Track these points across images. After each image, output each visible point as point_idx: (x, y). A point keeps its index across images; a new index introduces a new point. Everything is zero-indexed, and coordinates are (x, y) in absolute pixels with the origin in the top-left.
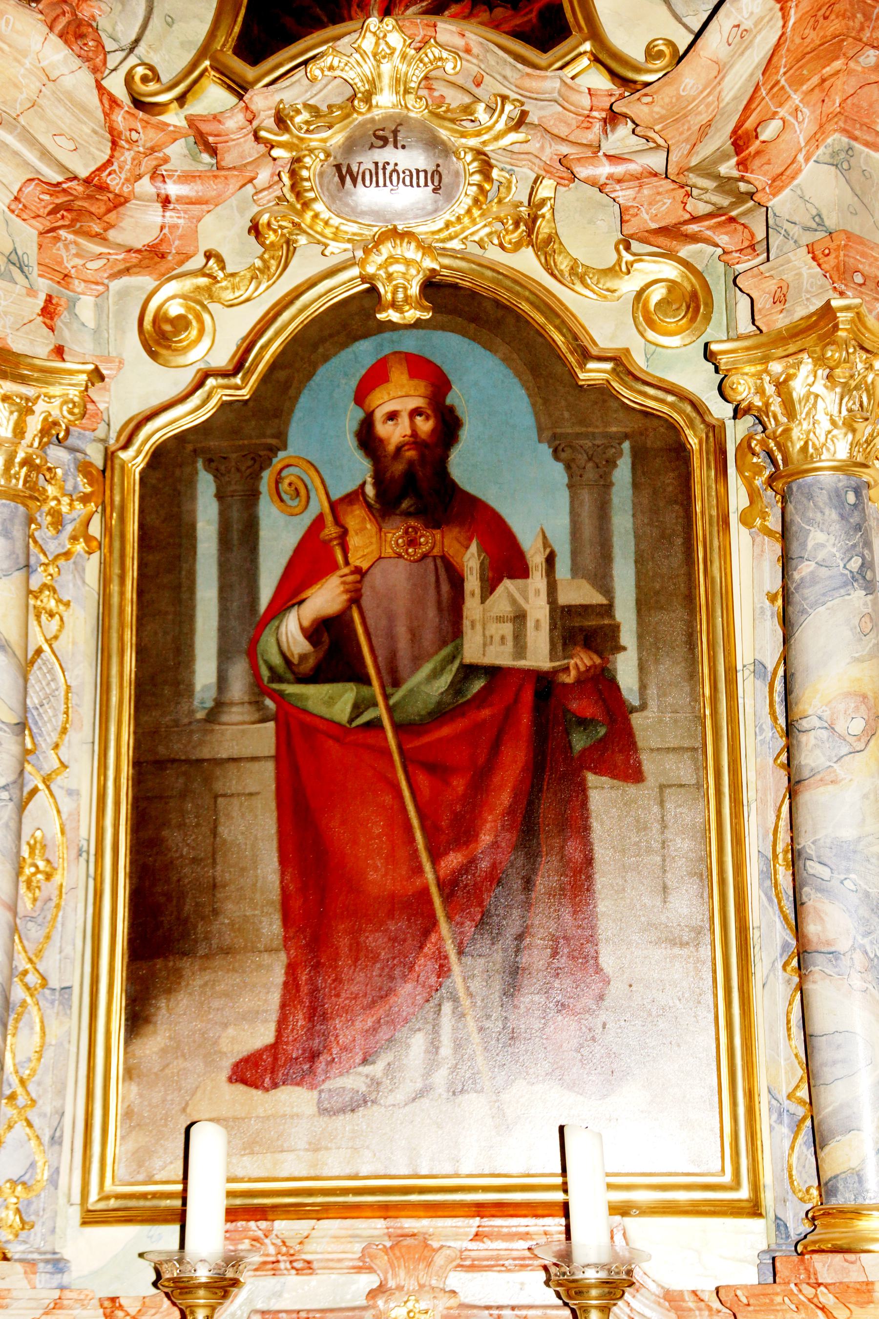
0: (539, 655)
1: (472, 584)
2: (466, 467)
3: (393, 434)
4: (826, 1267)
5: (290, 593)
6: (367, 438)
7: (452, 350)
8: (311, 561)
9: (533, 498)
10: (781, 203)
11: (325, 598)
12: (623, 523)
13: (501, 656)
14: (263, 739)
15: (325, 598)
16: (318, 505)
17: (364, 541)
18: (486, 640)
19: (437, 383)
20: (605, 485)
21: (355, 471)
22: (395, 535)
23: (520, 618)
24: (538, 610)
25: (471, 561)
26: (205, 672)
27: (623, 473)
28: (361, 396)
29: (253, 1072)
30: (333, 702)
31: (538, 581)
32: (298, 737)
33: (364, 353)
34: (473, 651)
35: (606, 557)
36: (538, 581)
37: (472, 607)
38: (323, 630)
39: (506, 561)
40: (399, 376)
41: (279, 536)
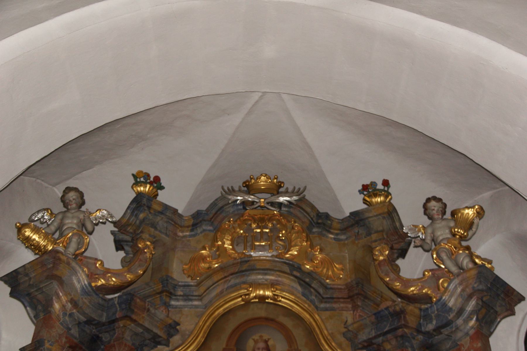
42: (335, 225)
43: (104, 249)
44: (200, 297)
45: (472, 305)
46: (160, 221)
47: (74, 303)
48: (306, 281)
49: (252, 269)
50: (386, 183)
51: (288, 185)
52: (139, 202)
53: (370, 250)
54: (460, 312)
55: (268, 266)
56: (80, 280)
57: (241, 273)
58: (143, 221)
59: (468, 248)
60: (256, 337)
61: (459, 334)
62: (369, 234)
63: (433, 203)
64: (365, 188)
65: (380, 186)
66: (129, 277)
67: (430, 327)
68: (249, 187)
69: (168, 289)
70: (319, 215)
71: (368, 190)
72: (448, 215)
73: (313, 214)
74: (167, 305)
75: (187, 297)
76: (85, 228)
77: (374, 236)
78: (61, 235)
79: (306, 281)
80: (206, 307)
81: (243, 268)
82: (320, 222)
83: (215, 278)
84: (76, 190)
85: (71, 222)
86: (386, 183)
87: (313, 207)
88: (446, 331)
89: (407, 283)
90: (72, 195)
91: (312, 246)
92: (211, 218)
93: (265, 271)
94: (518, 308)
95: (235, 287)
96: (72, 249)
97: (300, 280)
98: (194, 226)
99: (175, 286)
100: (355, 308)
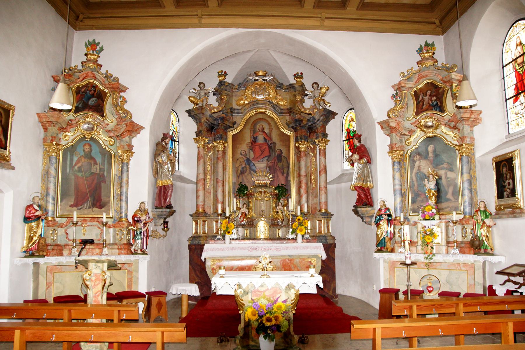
0: (98, 172)
1: (93, 165)
2: (93, 154)
3: (86, 150)
4: (120, 222)
5: (76, 165)
6: (84, 150)
7: (92, 143)
8: (78, 161)
9: (99, 159)
10: (124, 139)
11: (79, 165)
12: (106, 161)
13: (95, 172)
14: (73, 177)
15: (79, 165)
16: (79, 156)
17: (83, 160)
18: (93, 170)
19: (91, 146)
20: (105, 157)
21: (82, 153)
22: (86, 160)
23: (96, 169)
24: (98, 168)
25: (93, 163)
26: (68, 170)
27: (106, 156)
28: (84, 146)
29: (72, 206)
30: (80, 174)
31: (98, 165)
32: (77, 177)
33: (84, 143)
34: (92, 171)
35: (104, 164)
36: (98, 165)
37: (93, 167)
38: (79, 168)
39: (96, 163)
40: (87, 145)
41: (75, 159)
42: (285, 87)
43: (213, 101)
44: (242, 113)
45: (321, 118)
46: (228, 88)
47: (208, 120)
48: (275, 107)
49: (258, 104)
50: (302, 73)
51: (270, 73)
52: (221, 83)
53: (295, 96)
54: (318, 120)
55: (263, 102)
56: (208, 113)
57: (254, 105)
58: (222, 89)
59: (324, 100)
60: (260, 124)
61: (318, 126)
62: (295, 91)
63: (314, 85)
64: (295, 75)
65: (300, 74)
66: (220, 108)
67: (310, 124)
68: (256, 74)
69: (232, 110)
70: (279, 84)
71: (296, 76)
72: (319, 88)
73: (278, 83)
74: (232, 115)
75: (238, 113)
76: (207, 94)
77: (297, 92)
78: (200, 98)
79: (275, 107)
80: (244, 116)
81: (255, 103)
82: (279, 86)
83: (247, 106)
84: (203, 83)
85: (202, 94)
86: (302, 73)
87: (277, 81)
88: (314, 125)
89: (305, 109)
90: (202, 85)
91: (277, 94)
92: (243, 85)
93: (262, 104)
94: (336, 117)
95: (253, 109)
96: (204, 104)
97: (273, 108)
98: (238, 89)
99: (234, 110)
100: (290, 115)
